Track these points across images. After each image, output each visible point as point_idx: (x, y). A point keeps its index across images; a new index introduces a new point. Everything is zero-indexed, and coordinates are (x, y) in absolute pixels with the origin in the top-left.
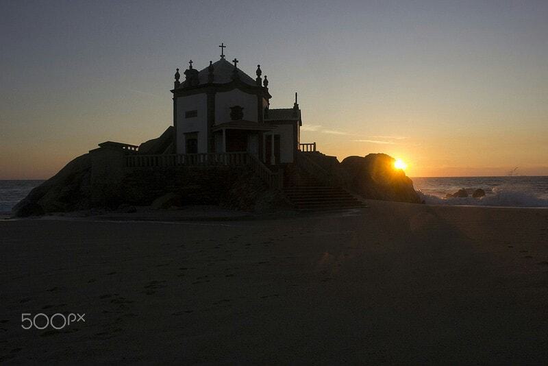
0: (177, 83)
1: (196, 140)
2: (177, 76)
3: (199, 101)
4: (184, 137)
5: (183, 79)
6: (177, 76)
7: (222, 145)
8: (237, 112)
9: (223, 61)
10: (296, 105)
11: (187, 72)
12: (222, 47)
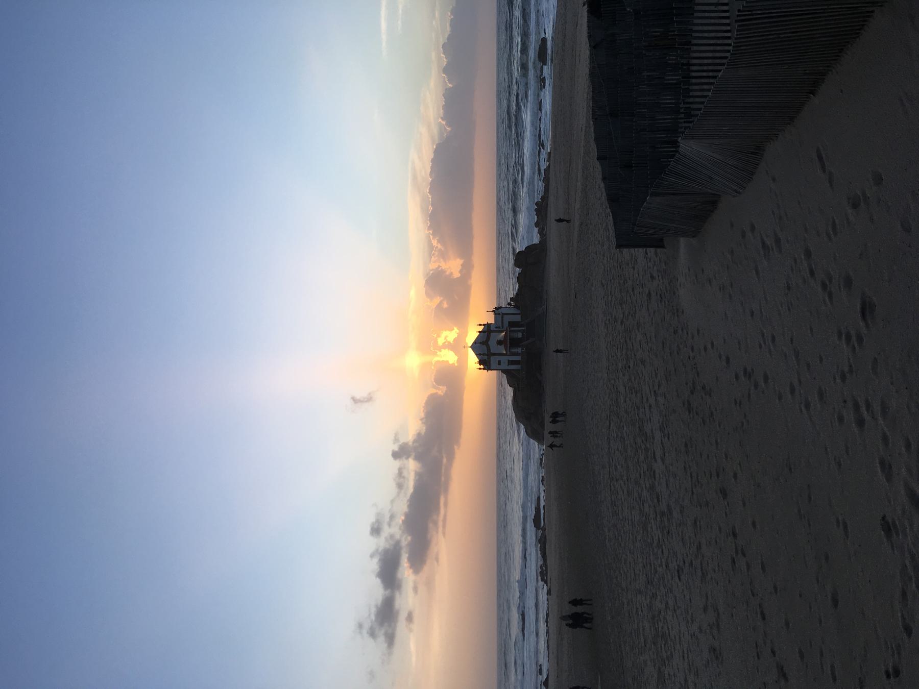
0: (484, 369)
1: (512, 361)
2: (480, 369)
3: (494, 360)
4: (509, 366)
5: (482, 367)
6: (480, 369)
7: (514, 350)
8: (500, 343)
9: (471, 347)
10: (493, 311)
11: (480, 365)
12: (464, 347)
